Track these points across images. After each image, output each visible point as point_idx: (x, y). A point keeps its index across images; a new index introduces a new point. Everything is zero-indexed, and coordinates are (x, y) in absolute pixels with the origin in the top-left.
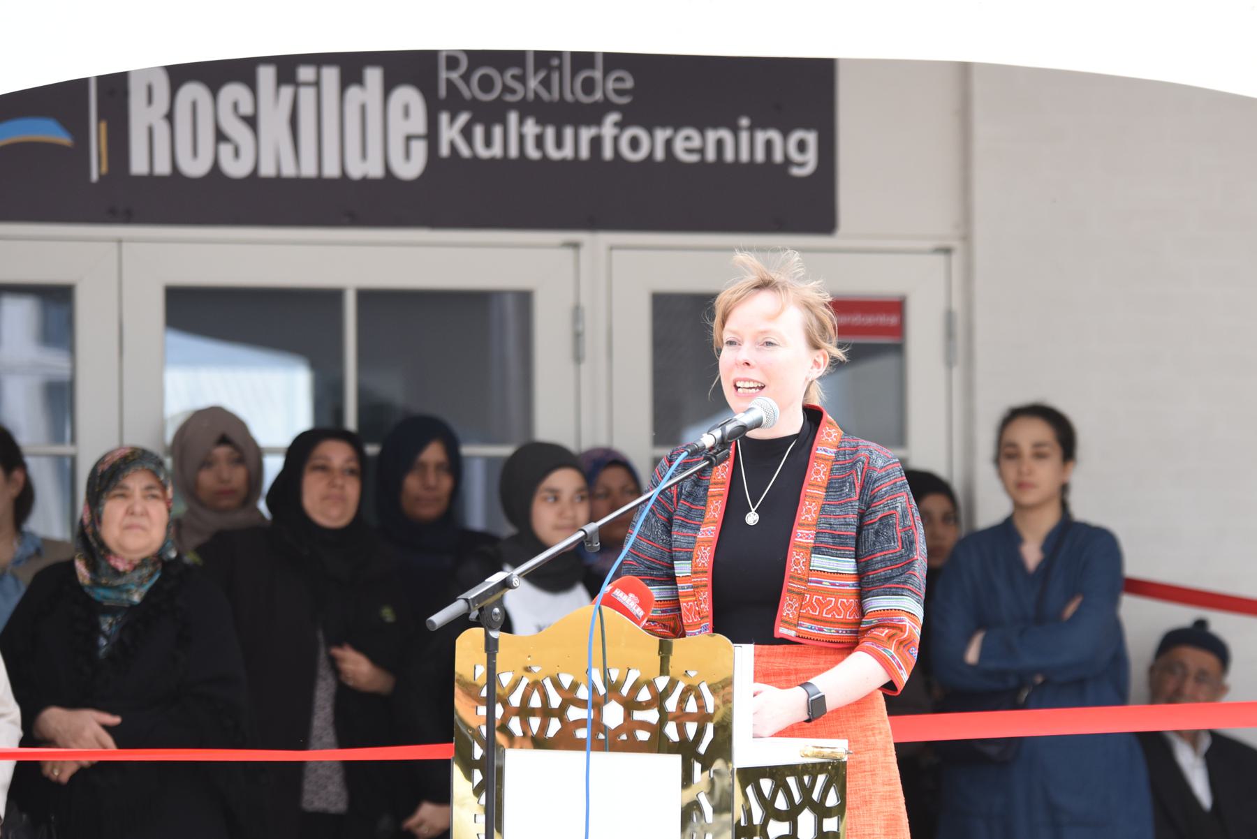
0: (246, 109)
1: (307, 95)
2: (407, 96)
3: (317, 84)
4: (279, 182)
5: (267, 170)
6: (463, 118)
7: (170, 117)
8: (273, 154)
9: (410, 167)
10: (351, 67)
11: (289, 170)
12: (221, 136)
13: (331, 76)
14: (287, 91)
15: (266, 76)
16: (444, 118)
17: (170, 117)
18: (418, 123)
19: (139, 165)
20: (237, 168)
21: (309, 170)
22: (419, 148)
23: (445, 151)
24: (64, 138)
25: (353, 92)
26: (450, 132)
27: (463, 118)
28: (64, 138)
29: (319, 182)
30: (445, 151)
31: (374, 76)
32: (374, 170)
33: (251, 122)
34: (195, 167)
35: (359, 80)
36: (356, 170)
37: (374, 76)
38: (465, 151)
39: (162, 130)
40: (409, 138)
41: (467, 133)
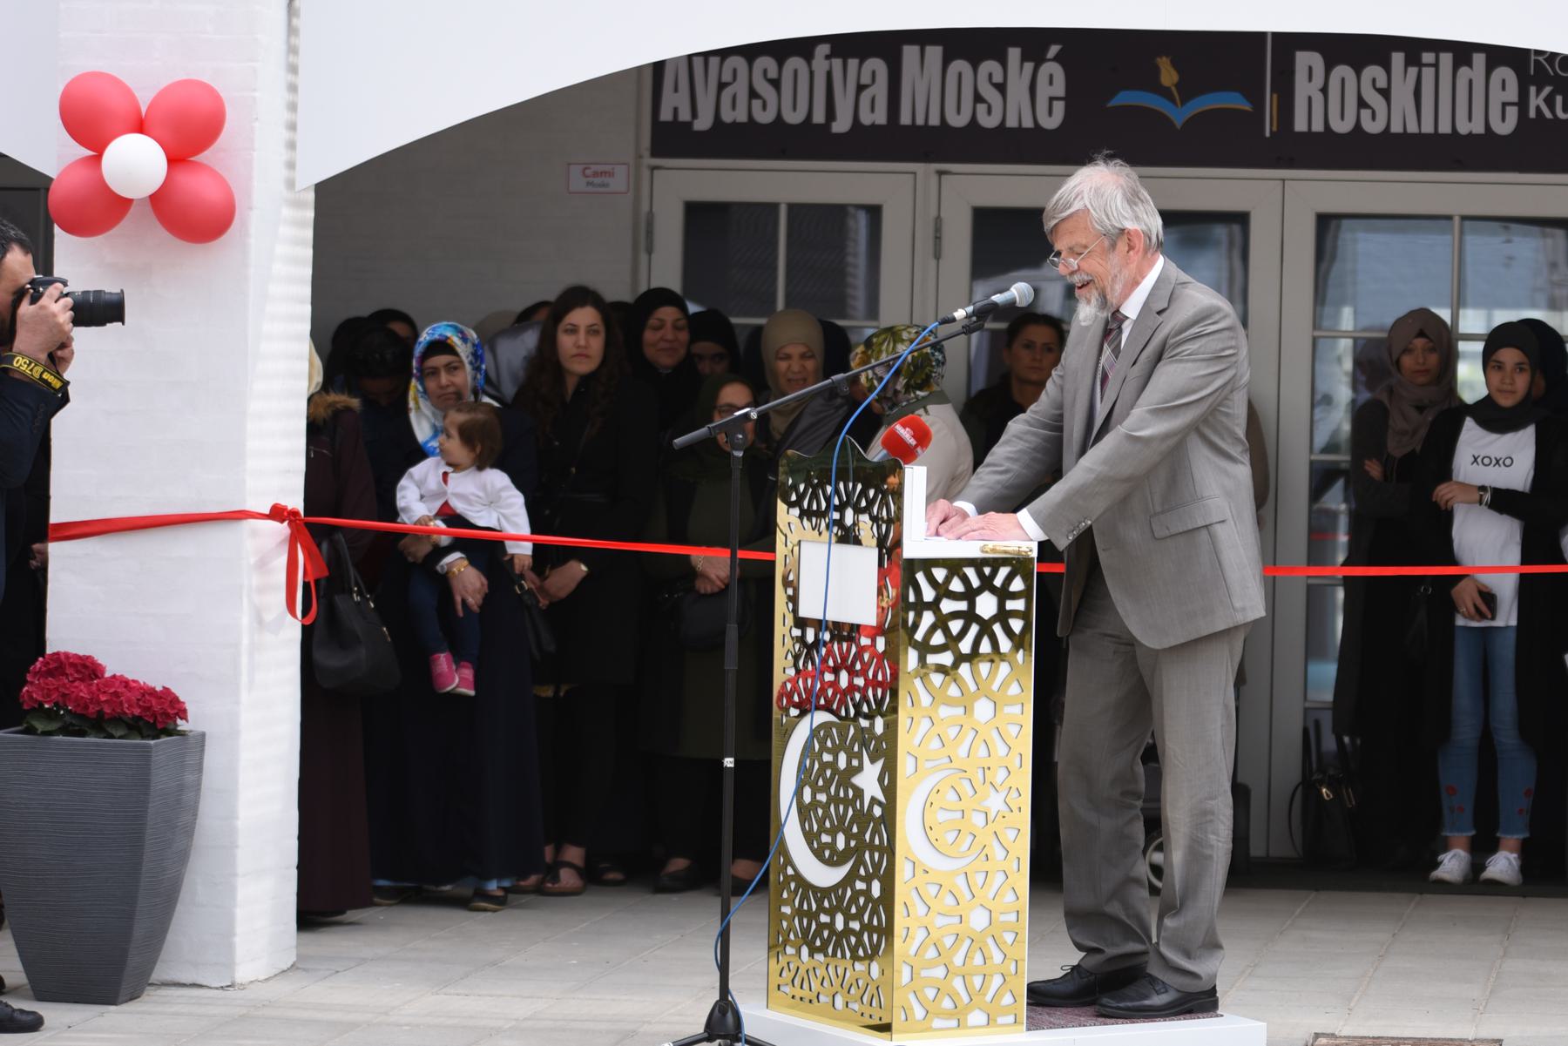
0: (1382, 83)
1: (1428, 74)
2: (1505, 73)
3: (1436, 65)
4: (1405, 136)
5: (1396, 128)
6: (1548, 90)
7: (1324, 90)
8: (1401, 117)
9: (1505, 126)
10: (1462, 52)
11: (1412, 128)
12: (1362, 104)
13: (1446, 59)
14: (1413, 71)
15: (1398, 58)
16: (1533, 89)
17: (1324, 90)
18: (1512, 94)
19: (1300, 125)
20: (1373, 127)
21: (1428, 128)
22: (1512, 113)
23: (1532, 114)
24: (1247, 107)
25: (1464, 72)
26: (1536, 101)
27: (1548, 90)
28: (1247, 107)
29: (1436, 136)
30: (1532, 114)
31: (1479, 59)
32: (1478, 128)
33: (1385, 93)
34: (1342, 127)
35: (1469, 64)
36: (1463, 129)
37: (1479, 59)
38: (1548, 115)
39: (1318, 99)
40: (1504, 105)
41: (1550, 101)
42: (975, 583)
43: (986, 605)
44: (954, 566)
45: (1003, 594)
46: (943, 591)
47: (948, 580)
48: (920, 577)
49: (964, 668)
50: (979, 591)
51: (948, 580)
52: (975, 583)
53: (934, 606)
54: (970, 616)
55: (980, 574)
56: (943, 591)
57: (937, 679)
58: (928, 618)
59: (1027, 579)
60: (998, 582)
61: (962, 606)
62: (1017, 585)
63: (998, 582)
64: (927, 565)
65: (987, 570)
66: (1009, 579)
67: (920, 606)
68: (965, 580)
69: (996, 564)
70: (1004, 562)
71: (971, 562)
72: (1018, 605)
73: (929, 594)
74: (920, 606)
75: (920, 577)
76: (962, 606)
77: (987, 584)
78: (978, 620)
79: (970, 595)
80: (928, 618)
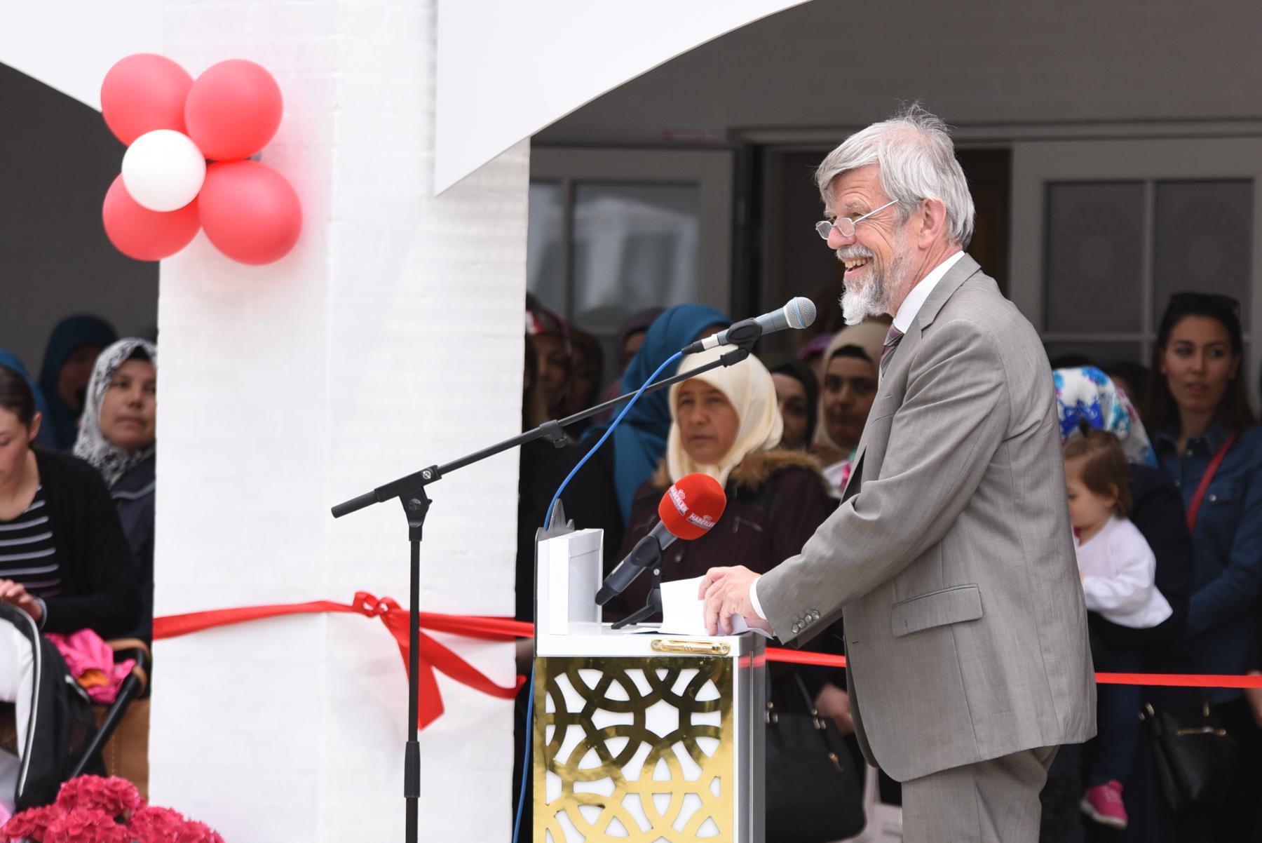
42: (645, 689)
43: (662, 719)
44: (613, 668)
45: (687, 705)
46: (596, 699)
47: (603, 685)
48: (562, 681)
49: (632, 804)
50: (651, 700)
51: (603, 685)
52: (645, 689)
53: (584, 719)
54: (637, 734)
55: (652, 679)
56: (596, 699)
57: (591, 814)
58: (575, 734)
59: (724, 685)
60: (679, 688)
61: (627, 719)
62: (709, 692)
63: (679, 688)
64: (569, 665)
65: (662, 674)
66: (695, 685)
67: (563, 719)
68: (630, 686)
69: (675, 665)
70: (688, 662)
71: (635, 662)
72: (713, 719)
73: (575, 703)
74: (563, 719)
75: (562, 681)
76: (627, 719)
77: (662, 691)
78: (652, 738)
79: (637, 705)
80: (575, 734)
